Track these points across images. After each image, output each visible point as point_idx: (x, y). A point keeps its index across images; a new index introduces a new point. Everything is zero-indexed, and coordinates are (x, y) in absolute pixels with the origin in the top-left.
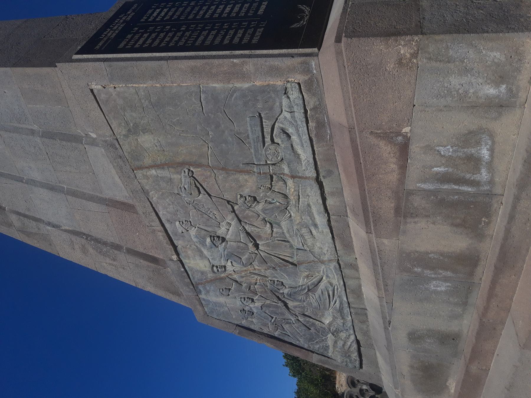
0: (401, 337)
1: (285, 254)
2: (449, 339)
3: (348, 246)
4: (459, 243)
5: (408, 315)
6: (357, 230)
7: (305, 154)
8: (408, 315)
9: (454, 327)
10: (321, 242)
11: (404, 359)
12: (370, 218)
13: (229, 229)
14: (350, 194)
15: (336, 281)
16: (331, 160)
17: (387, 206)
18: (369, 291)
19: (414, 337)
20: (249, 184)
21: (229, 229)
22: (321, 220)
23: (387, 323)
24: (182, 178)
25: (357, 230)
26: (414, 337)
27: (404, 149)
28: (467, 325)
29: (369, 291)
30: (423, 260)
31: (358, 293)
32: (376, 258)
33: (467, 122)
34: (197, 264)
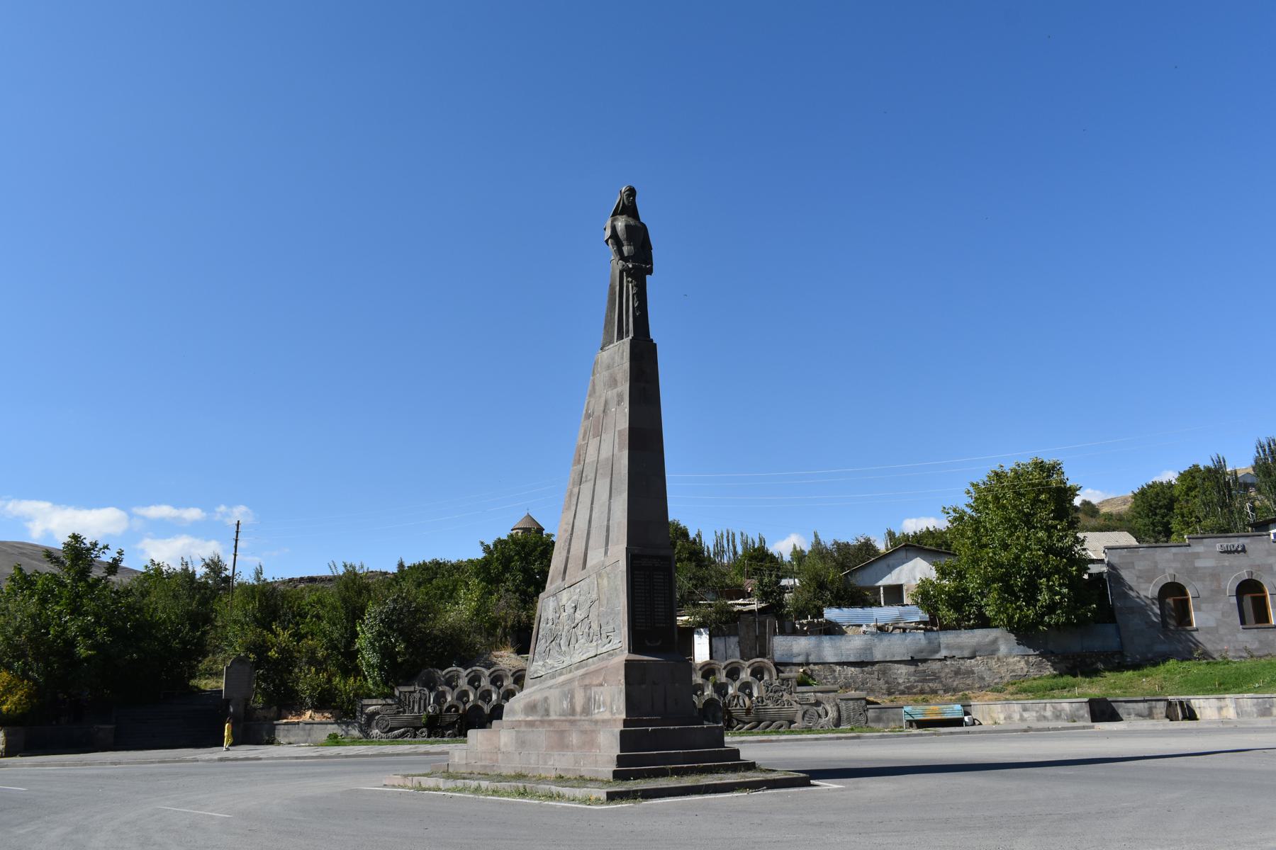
0: (546, 694)
1: (573, 641)
2: (547, 713)
3: (577, 668)
4: (578, 709)
5: (554, 695)
6: (581, 671)
7: (604, 650)
8: (554, 695)
9: (552, 713)
10: (577, 658)
11: (538, 697)
12: (584, 676)
13: (579, 615)
14: (592, 668)
15: (565, 664)
16: (603, 659)
17: (587, 682)
18: (562, 679)
19: (546, 699)
20: (595, 626)
21: (579, 615)
22: (584, 657)
23: (550, 688)
24: (594, 596)
25: (581, 671)
26: (546, 699)
27: (601, 685)
28: (553, 717)
29: (562, 679)
30: (572, 697)
31: (561, 674)
32: (570, 681)
33: (608, 704)
34: (564, 596)
